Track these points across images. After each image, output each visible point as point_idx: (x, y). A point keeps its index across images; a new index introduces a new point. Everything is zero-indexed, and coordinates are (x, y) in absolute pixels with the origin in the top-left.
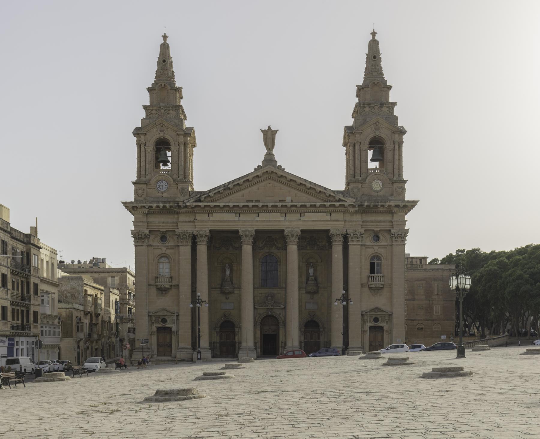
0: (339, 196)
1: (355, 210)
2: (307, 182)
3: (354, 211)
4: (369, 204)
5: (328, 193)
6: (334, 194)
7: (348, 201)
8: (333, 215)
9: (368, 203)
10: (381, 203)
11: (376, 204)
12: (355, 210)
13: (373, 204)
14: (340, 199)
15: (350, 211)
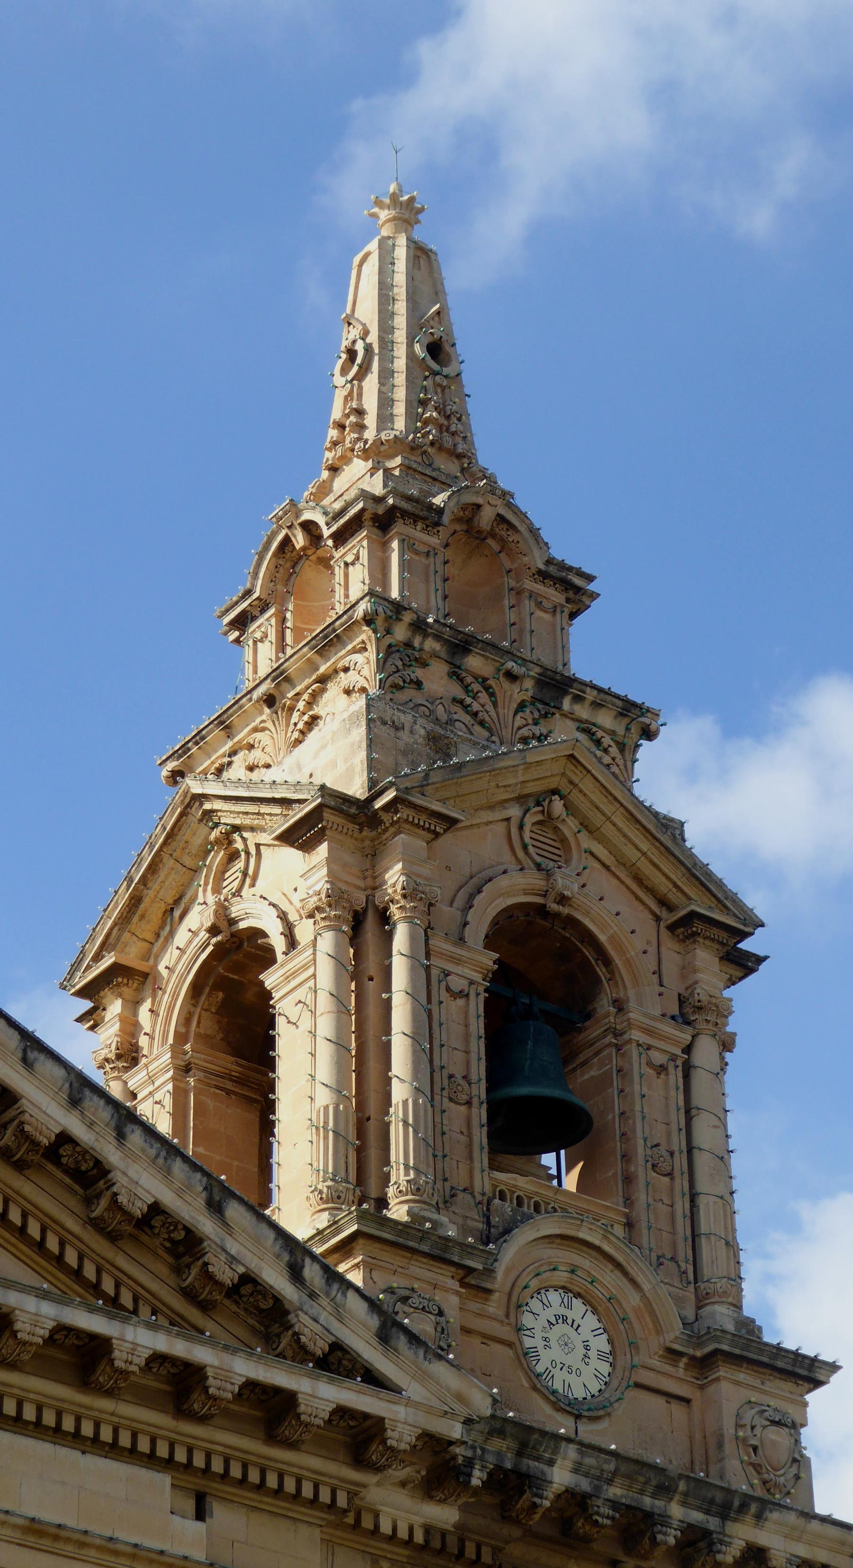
0: (339, 1312)
1: (428, 1530)
2: (45, 1066)
3: (419, 1538)
4: (585, 1485)
5: (233, 1248)
6: (296, 1274)
7: (414, 1390)
8: (219, 1512)
9: (576, 1471)
10: (684, 1504)
11: (647, 1502)
12: (428, 1530)
13: (615, 1491)
14: (337, 1347)
15: (386, 1527)
